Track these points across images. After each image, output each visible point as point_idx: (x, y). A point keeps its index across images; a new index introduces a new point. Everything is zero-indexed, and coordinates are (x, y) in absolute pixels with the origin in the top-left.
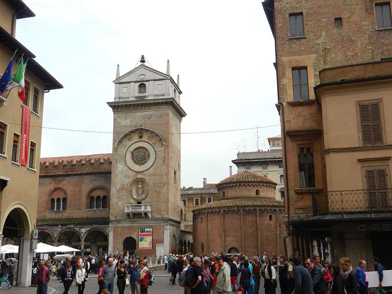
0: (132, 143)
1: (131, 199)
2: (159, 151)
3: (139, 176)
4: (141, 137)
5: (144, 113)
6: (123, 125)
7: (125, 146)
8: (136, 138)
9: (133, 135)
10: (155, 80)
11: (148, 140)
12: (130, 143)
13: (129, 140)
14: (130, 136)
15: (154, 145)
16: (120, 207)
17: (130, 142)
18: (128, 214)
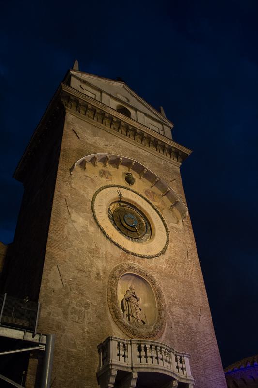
0: (110, 183)
1: (113, 325)
2: (173, 228)
3: (136, 264)
4: (129, 180)
5: (133, 148)
6: (88, 142)
7: (92, 180)
8: (118, 175)
9: (110, 168)
10: (146, 115)
11: (147, 196)
12: (104, 181)
13: (103, 173)
14: (104, 169)
15: (162, 213)
16: (75, 346)
17: (103, 179)
18: (123, 376)
